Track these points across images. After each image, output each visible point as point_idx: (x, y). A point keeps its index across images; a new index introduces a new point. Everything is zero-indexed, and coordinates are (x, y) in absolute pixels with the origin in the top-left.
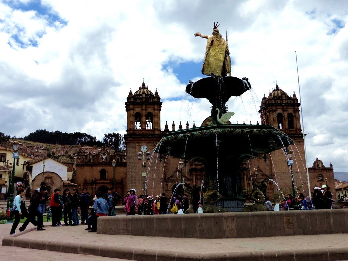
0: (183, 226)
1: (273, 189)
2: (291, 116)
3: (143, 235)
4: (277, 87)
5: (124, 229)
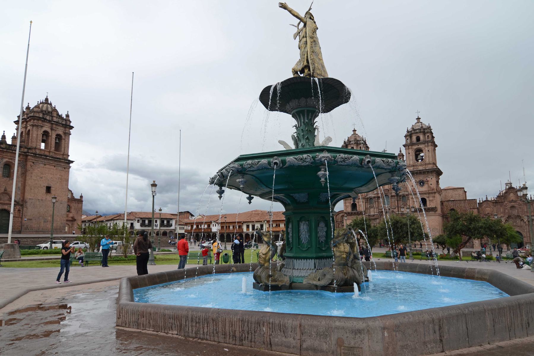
1: (22, 218)
2: (59, 137)
4: (47, 99)
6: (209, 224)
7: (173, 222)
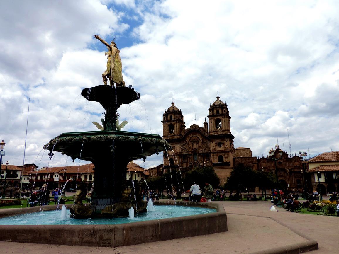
0: (207, 224)
3: (173, 239)
5: (152, 236)
6: (52, 175)
7: (19, 174)
